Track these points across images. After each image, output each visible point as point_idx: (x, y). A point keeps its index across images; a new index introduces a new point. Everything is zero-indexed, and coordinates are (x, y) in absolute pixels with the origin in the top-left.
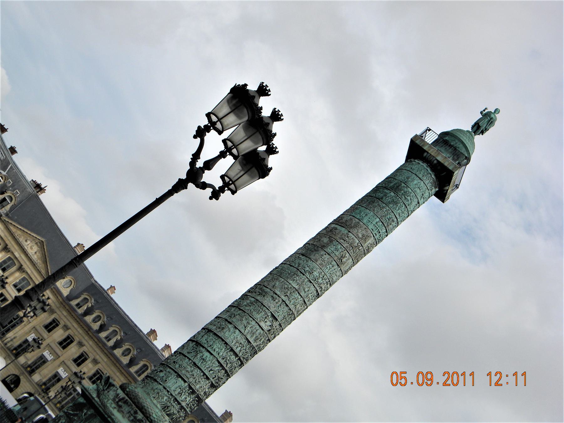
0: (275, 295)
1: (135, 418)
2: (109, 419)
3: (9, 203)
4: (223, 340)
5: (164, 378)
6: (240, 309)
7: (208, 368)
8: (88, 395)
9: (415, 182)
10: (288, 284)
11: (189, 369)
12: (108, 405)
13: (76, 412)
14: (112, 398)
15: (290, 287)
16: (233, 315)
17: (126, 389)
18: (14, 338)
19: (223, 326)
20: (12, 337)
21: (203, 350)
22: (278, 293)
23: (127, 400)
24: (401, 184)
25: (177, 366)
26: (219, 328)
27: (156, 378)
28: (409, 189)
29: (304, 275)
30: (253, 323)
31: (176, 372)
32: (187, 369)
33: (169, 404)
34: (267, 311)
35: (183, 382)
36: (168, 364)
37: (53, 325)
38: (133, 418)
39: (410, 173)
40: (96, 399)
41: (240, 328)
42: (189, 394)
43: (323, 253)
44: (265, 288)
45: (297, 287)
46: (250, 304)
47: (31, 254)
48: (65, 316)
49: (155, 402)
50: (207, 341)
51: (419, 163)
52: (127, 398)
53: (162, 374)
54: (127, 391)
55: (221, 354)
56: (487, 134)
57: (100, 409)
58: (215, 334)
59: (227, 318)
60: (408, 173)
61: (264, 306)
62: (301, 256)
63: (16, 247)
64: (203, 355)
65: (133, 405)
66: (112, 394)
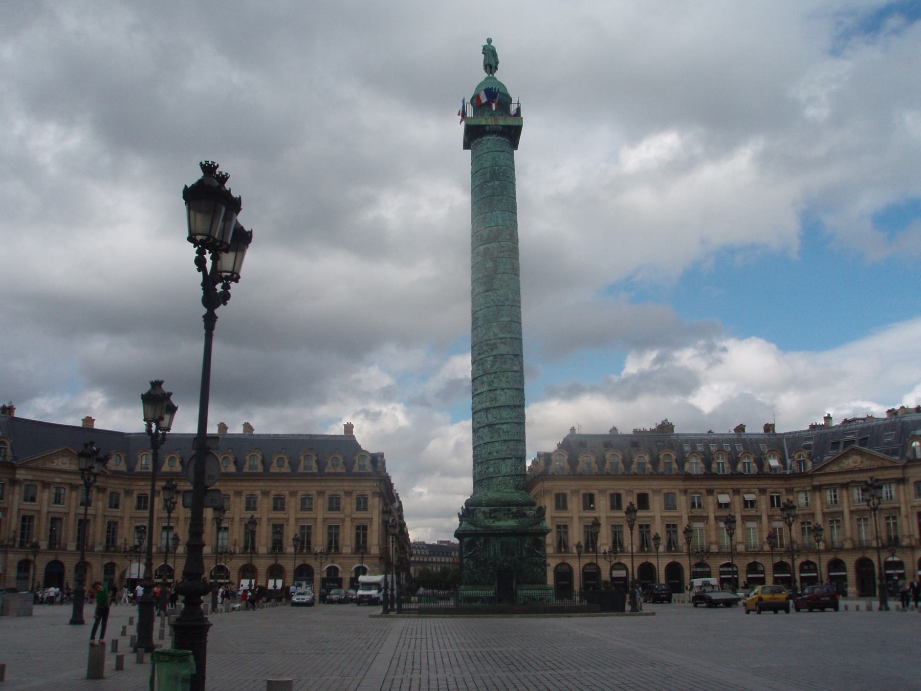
0: (503, 340)
1: (513, 513)
2: (501, 532)
3: (6, 448)
4: (504, 406)
5: (496, 470)
6: (491, 374)
7: (515, 434)
8: (470, 532)
9: (502, 158)
10: (501, 323)
11: (505, 448)
12: (488, 524)
13: (473, 550)
14: (483, 518)
15: (505, 323)
16: (491, 383)
17: (481, 502)
18: (126, 540)
19: (493, 397)
20: (123, 542)
21: (499, 426)
22: (503, 336)
23: (494, 509)
24: (495, 169)
25: (495, 454)
26: (492, 401)
27: (490, 476)
28: (503, 167)
29: (504, 305)
30: (510, 374)
31: (499, 459)
32: (504, 449)
33: (517, 483)
34: (508, 356)
35: (510, 460)
36: (486, 459)
37: (752, 533)
38: (511, 515)
39: (491, 153)
40: (478, 529)
41: (505, 386)
42: (520, 463)
43: (500, 276)
44: (489, 342)
45: (509, 319)
46: (494, 363)
47: (68, 469)
48: (144, 485)
49: (508, 490)
50: (495, 418)
51: (489, 139)
52: (493, 508)
53: (491, 470)
54: (484, 504)
55: (512, 416)
56: (499, 66)
57: (488, 532)
58: (494, 408)
59: (488, 389)
60: (489, 155)
61: (504, 355)
62: (487, 294)
63: (52, 475)
64: (503, 429)
65: (502, 507)
66: (480, 516)
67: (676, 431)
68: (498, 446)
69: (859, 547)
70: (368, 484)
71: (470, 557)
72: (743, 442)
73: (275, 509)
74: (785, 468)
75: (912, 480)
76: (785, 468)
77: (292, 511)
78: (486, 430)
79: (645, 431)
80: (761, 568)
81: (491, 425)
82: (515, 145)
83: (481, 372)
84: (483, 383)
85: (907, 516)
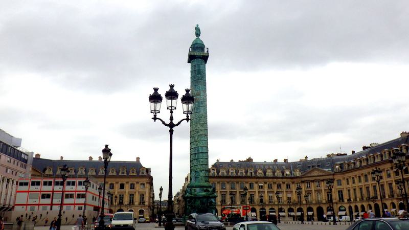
11: (201, 167)
67: (253, 161)
68: (199, 167)
69: (318, 202)
70: (144, 179)
71: (189, 206)
72: (277, 165)
73: (131, 188)
74: (291, 175)
75: (336, 180)
76: (291, 175)
77: (116, 189)
78: (195, 161)
79: (243, 161)
80: (283, 210)
81: (196, 159)
82: (206, 62)
83: (194, 141)
84: (194, 144)
85: (334, 192)
